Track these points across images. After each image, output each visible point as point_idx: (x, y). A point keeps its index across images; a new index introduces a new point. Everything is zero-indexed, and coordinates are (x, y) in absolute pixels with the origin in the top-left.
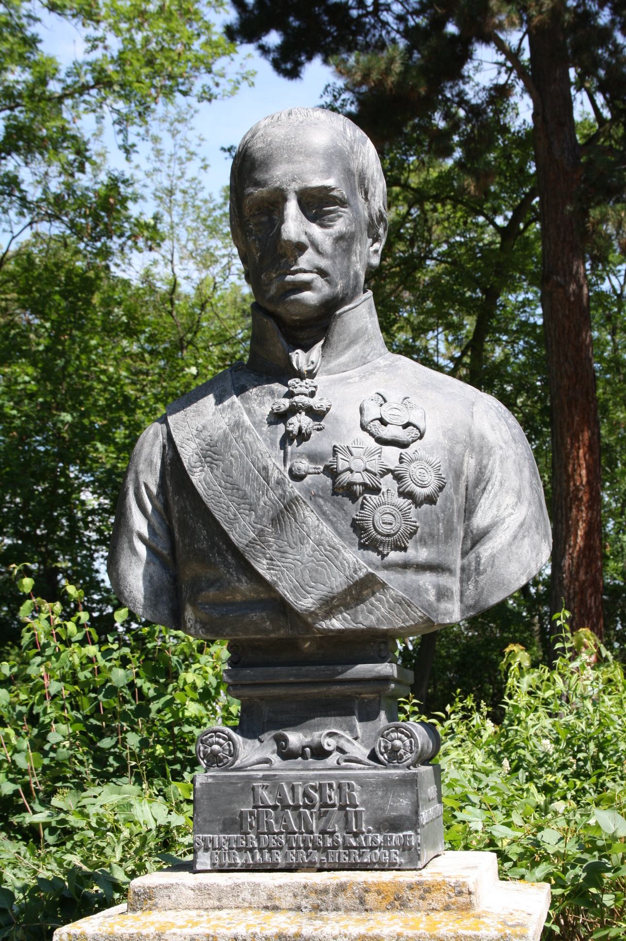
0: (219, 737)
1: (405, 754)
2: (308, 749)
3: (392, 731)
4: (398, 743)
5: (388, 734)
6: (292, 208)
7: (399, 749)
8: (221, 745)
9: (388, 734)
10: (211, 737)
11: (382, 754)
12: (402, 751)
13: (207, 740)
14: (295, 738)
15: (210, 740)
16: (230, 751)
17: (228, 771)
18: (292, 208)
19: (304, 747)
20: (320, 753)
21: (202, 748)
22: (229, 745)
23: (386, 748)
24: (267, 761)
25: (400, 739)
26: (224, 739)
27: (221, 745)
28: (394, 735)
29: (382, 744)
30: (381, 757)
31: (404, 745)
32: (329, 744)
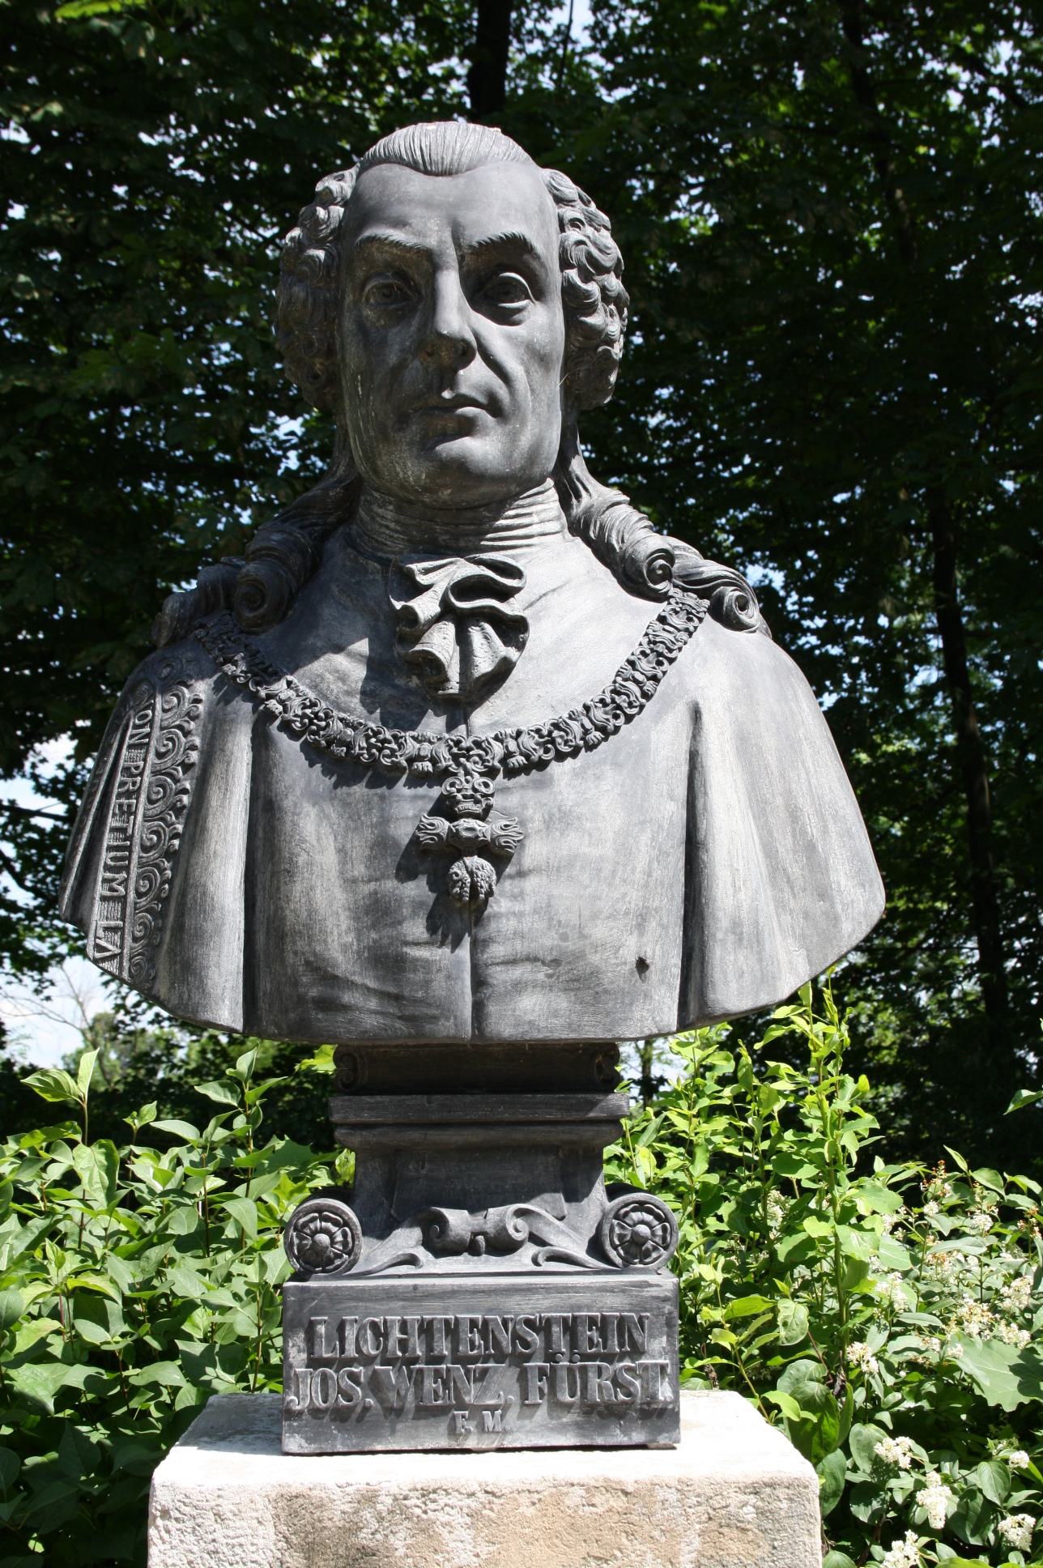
0: (327, 1219)
1: (655, 1249)
2: (480, 1238)
3: (634, 1210)
4: (643, 1230)
5: (626, 1214)
6: (450, 284)
7: (646, 1240)
8: (331, 1235)
9: (626, 1214)
10: (313, 1220)
11: (615, 1248)
12: (650, 1244)
13: (305, 1225)
14: (458, 1220)
15: (312, 1226)
16: (345, 1243)
17: (340, 1277)
18: (450, 284)
19: (475, 1234)
20: (502, 1245)
21: (296, 1241)
22: (345, 1235)
23: (621, 1237)
24: (412, 1260)
25: (643, 1222)
26: (336, 1223)
27: (331, 1235)
28: (636, 1216)
29: (617, 1230)
30: (613, 1254)
31: (653, 1234)
32: (517, 1229)
